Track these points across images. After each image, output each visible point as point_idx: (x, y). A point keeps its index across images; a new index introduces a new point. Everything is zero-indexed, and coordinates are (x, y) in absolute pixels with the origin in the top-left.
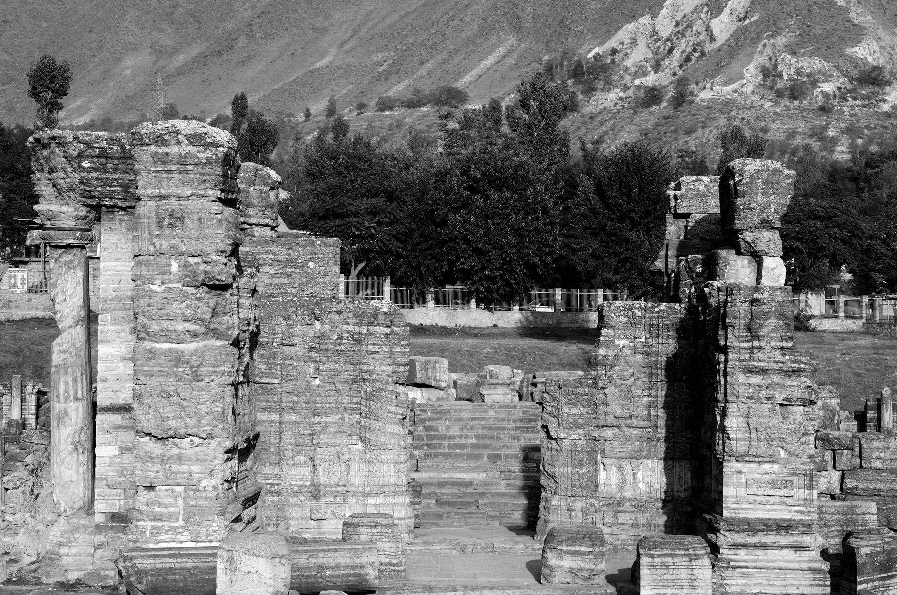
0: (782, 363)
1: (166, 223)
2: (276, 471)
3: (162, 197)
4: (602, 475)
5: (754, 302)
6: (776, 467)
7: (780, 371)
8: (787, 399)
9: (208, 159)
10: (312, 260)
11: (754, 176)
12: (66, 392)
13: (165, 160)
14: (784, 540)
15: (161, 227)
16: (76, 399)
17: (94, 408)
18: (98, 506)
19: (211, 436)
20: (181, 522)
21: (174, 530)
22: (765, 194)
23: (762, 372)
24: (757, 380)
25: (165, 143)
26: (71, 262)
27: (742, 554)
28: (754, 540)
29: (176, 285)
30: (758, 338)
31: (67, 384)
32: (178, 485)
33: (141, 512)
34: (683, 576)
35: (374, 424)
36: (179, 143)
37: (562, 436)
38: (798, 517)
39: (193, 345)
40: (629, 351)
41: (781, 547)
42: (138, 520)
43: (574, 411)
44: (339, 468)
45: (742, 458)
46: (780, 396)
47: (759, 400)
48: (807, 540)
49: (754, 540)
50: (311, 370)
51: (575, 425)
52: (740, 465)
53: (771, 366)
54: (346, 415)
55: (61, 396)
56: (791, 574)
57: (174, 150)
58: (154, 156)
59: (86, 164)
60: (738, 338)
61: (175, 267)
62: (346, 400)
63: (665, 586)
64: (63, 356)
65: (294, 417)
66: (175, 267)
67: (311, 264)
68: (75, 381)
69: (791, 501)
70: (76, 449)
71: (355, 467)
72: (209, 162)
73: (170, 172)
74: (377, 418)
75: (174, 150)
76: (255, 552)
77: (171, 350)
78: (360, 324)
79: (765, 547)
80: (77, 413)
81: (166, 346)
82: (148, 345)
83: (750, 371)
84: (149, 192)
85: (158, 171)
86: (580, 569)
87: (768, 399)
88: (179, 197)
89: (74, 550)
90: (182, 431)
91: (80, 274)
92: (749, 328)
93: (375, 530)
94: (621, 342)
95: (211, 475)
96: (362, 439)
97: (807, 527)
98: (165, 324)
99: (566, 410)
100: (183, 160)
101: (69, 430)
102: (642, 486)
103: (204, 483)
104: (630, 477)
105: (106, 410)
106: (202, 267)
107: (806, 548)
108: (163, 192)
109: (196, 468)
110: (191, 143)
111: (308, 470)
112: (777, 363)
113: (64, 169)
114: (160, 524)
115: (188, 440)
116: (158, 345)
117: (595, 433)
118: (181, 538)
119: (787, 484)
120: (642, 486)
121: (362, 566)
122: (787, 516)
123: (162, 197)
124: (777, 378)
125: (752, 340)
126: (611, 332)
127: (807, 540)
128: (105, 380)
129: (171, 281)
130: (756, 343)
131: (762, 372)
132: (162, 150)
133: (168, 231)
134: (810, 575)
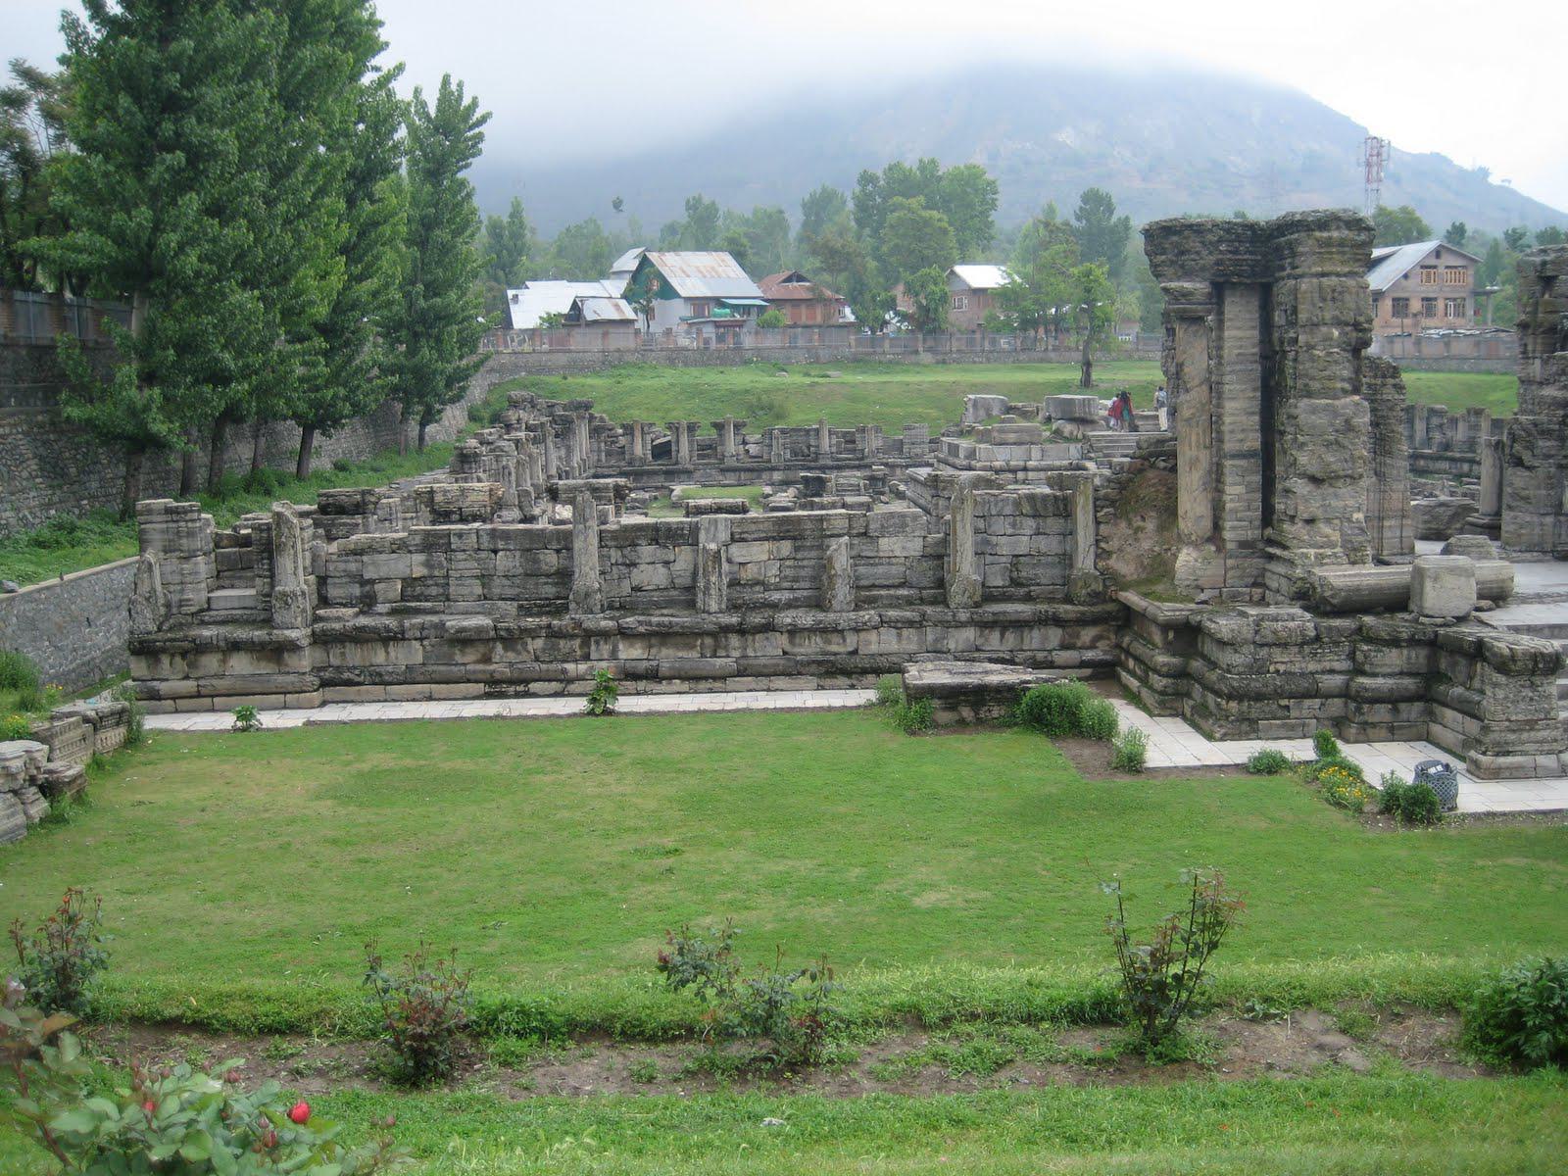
3: (1323, 275)
12: (1198, 441)
13: (1328, 243)
15: (1324, 300)
18: (1227, 535)
21: (1335, 554)
36: (1338, 228)
43: (1549, 444)
51: (1548, 457)
57: (1335, 234)
59: (1223, 247)
66: (1336, 333)
73: (1331, 253)
78: (1375, 377)
88: (1338, 275)
90: (1341, 473)
99: (1540, 443)
100: (1342, 243)
113: (1198, 253)
129: (1331, 346)
132: (1325, 234)
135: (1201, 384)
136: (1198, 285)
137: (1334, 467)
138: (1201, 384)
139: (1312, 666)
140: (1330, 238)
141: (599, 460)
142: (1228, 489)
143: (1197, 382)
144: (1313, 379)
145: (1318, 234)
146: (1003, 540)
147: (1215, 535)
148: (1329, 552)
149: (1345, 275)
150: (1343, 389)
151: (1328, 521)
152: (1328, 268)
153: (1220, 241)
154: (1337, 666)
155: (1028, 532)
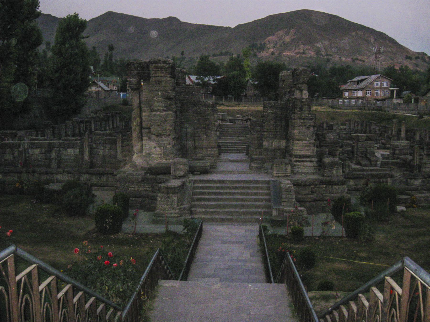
2: (186, 142)
3: (157, 77)
4: (264, 143)
5: (302, 102)
6: (306, 142)
7: (308, 119)
11: (301, 71)
13: (157, 67)
14: (308, 159)
16: (138, 126)
17: (142, 128)
19: (169, 135)
20: (163, 156)
23: (304, 119)
24: (302, 121)
25: (157, 64)
27: (298, 164)
28: (301, 159)
30: (302, 110)
35: (209, 131)
36: (161, 63)
39: (164, 113)
40: (270, 114)
41: (307, 161)
44: (201, 142)
46: (308, 125)
47: (302, 126)
48: (313, 159)
49: (301, 159)
50: (194, 118)
52: (297, 142)
57: (159, 65)
58: (155, 66)
60: (298, 111)
61: (160, 93)
62: (202, 125)
66: (160, 93)
71: (205, 141)
72: (168, 68)
74: (210, 130)
75: (159, 65)
79: (303, 161)
80: (138, 128)
81: (158, 113)
82: (154, 113)
83: (300, 119)
88: (161, 77)
90: (162, 134)
91: (138, 95)
92: (300, 108)
94: (269, 111)
95: (169, 144)
97: (313, 157)
100: (161, 68)
101: (136, 133)
102: (274, 146)
103: (168, 146)
104: (270, 144)
105: (144, 128)
106: (166, 94)
109: (166, 143)
110: (163, 63)
117: (263, 133)
120: (274, 146)
121: (206, 166)
123: (157, 77)
127: (313, 159)
128: (144, 121)
129: (159, 97)
131: (304, 119)
133: (158, 85)
134: (313, 168)
136: (134, 80)
138: (137, 108)
139: (141, 189)
141: (122, 128)
143: (136, 107)
145: (154, 65)
152: (158, 75)
153: (138, 67)
154: (148, 189)
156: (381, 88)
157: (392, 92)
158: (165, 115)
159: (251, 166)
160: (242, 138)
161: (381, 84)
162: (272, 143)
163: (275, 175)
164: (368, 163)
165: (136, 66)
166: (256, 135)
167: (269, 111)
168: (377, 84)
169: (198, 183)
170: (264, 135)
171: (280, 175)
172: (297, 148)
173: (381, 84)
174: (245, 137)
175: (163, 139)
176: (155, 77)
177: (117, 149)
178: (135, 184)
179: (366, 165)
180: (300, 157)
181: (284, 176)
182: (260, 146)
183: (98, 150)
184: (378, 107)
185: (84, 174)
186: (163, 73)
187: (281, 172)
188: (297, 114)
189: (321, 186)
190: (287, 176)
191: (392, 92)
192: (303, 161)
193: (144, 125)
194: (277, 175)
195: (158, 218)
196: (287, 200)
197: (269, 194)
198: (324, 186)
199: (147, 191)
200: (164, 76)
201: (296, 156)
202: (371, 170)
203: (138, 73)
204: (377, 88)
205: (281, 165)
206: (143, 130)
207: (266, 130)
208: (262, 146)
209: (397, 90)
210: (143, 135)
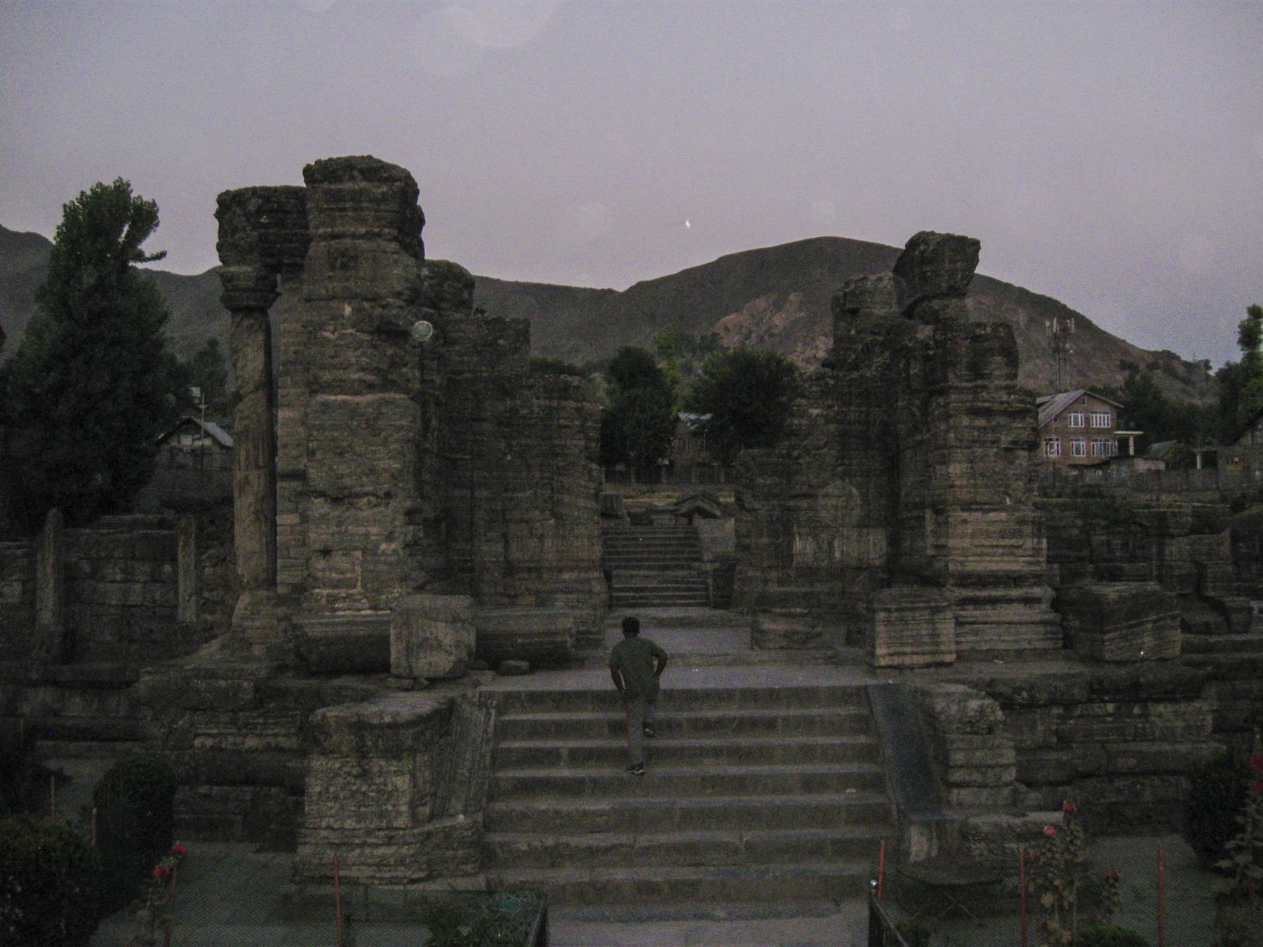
0: (1008, 402)
1: (338, 263)
3: (335, 236)
4: (798, 544)
6: (1003, 515)
7: (1004, 413)
8: (1013, 442)
9: (383, 194)
10: (501, 337)
13: (336, 197)
14: (1015, 593)
16: (258, 467)
17: (273, 477)
19: (388, 495)
20: (359, 589)
21: (349, 596)
22: (952, 262)
23: (988, 413)
24: (981, 422)
25: (338, 179)
26: (252, 325)
28: (984, 593)
29: (350, 331)
30: (982, 376)
31: (247, 451)
32: (356, 548)
33: (316, 579)
34: (924, 632)
36: (352, 178)
37: (757, 506)
38: (1027, 569)
39: (369, 398)
40: (822, 421)
41: (1010, 601)
42: (314, 588)
44: (533, 542)
45: (967, 507)
46: (1005, 439)
47: (982, 444)
48: (1036, 591)
49: (984, 593)
50: (503, 445)
52: (965, 515)
53: (996, 407)
54: (539, 491)
55: (243, 464)
56: (1023, 629)
57: (348, 185)
58: (325, 193)
59: (264, 220)
60: (960, 378)
62: (537, 474)
63: (902, 644)
64: (245, 422)
65: (485, 493)
66: (348, 310)
67: (501, 342)
68: (256, 448)
69: (1020, 551)
70: (258, 519)
71: (548, 543)
72: (384, 198)
73: (343, 209)
75: (348, 185)
76: (434, 615)
77: (344, 402)
79: (994, 601)
80: (257, 481)
81: (340, 398)
82: (321, 398)
83: (975, 412)
84: (321, 231)
85: (331, 209)
86: (794, 633)
87: (994, 442)
88: (354, 236)
89: (257, 624)
90: (358, 489)
91: (261, 337)
93: (570, 596)
94: (815, 412)
95: (390, 538)
96: (555, 515)
97: (1038, 579)
98: (340, 374)
100: (357, 196)
101: (251, 499)
103: (383, 546)
106: (378, 311)
107: (1037, 600)
108: (336, 230)
109: (374, 530)
110: (365, 179)
111: (500, 547)
112: (1002, 403)
114: (336, 591)
115: (365, 500)
116: (333, 398)
117: (792, 503)
118: (358, 605)
119: (1017, 534)
120: (837, 555)
122: (1016, 567)
123: (335, 236)
124: (1002, 420)
125: (974, 380)
126: (804, 401)
127: (1036, 591)
128: (285, 446)
130: (980, 382)
131: (988, 413)
134: (1041, 629)
135: (257, 389)
137: (347, 481)
138: (257, 389)
139: (251, 742)
140: (340, 191)
142: (280, 519)
143: (251, 387)
144: (322, 368)
146: (115, 586)
147: (272, 582)
148: (342, 593)
149: (362, 237)
150: (362, 381)
151: (347, 552)
152: (339, 229)
153: (259, 212)
154: (284, 742)
155: (142, 578)
156: (1088, 432)
157: (1123, 443)
158: (370, 404)
159: (762, 632)
160: (680, 573)
161: (1087, 420)
162: (830, 544)
163: (883, 662)
164: (1212, 618)
165: (252, 207)
166: (763, 512)
167: (815, 412)
168: (1076, 418)
169: (524, 710)
170: (798, 508)
171: (907, 660)
172: (966, 543)
173: (1087, 420)
174: (690, 568)
175: (362, 514)
176: (324, 237)
177: (176, 582)
178: (224, 718)
179: (1207, 629)
180: (982, 581)
181: (928, 666)
182: (783, 555)
183: (101, 586)
184: (1089, 486)
185: (34, 684)
186: (364, 221)
187: (908, 649)
188: (960, 390)
189: (1096, 709)
190: (941, 664)
191: (1123, 443)
192: (994, 601)
193: (281, 464)
194: (897, 661)
195: (312, 890)
196: (976, 776)
197: (868, 753)
198: (1110, 707)
199: (281, 750)
200: (369, 236)
201: (965, 580)
202: (1237, 647)
203: (262, 238)
204: (1076, 432)
205: (909, 614)
206: (279, 484)
207: (805, 489)
208: (790, 556)
209: (1137, 438)
210: (279, 507)
